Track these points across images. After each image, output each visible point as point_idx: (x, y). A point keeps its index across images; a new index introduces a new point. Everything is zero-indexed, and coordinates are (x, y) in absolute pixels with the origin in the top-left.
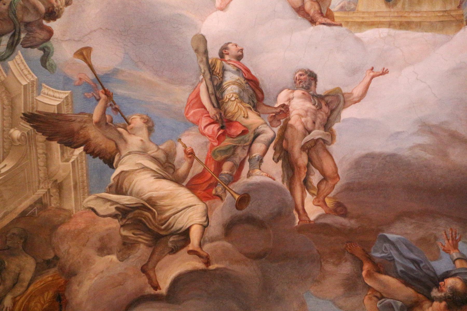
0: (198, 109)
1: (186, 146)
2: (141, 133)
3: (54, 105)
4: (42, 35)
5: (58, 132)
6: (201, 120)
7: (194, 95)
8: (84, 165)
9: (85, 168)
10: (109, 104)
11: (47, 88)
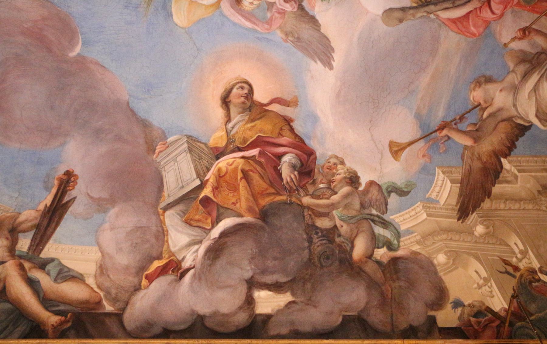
0: (470, 21)
1: (514, 38)
2: (491, 91)
3: (451, 186)
4: (374, 193)
5: (482, 186)
6: (485, 18)
7: (453, 26)
8: (523, 159)
9: (528, 158)
10: (454, 126)
11: (432, 192)
